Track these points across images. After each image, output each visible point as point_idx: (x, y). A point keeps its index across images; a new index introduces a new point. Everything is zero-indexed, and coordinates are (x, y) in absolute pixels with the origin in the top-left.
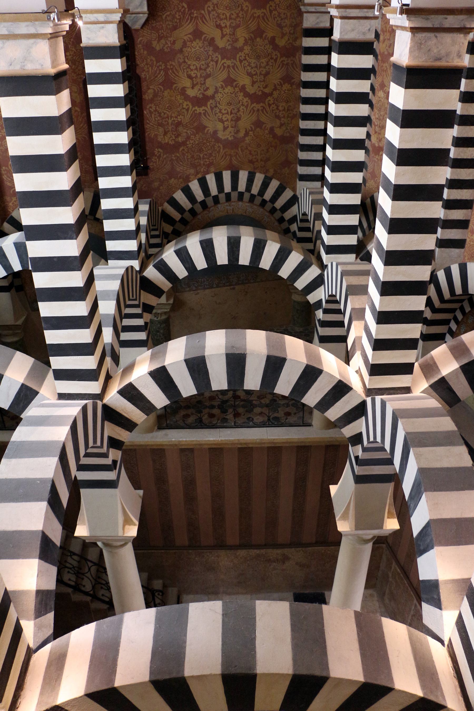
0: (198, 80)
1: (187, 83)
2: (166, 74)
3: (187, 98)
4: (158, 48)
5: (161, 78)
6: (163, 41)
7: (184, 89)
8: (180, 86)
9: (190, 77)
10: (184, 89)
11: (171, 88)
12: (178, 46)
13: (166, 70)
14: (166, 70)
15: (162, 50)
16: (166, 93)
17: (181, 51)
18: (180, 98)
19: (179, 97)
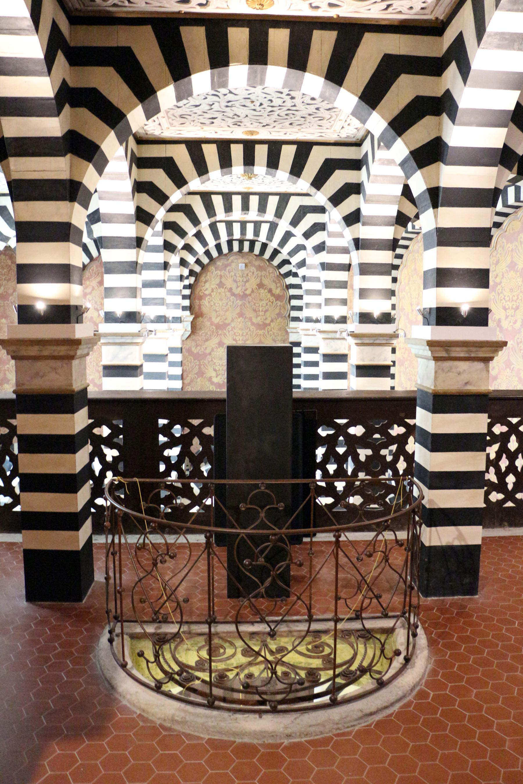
0: (220, 372)
1: (213, 374)
2: (200, 368)
3: (212, 383)
4: (195, 352)
5: (196, 370)
6: (199, 348)
7: (210, 378)
8: (208, 375)
9: (215, 370)
10: (210, 378)
11: (202, 376)
12: (208, 351)
13: (200, 365)
14: (200, 365)
15: (198, 353)
16: (199, 379)
17: (210, 354)
18: (208, 384)
19: (207, 383)
